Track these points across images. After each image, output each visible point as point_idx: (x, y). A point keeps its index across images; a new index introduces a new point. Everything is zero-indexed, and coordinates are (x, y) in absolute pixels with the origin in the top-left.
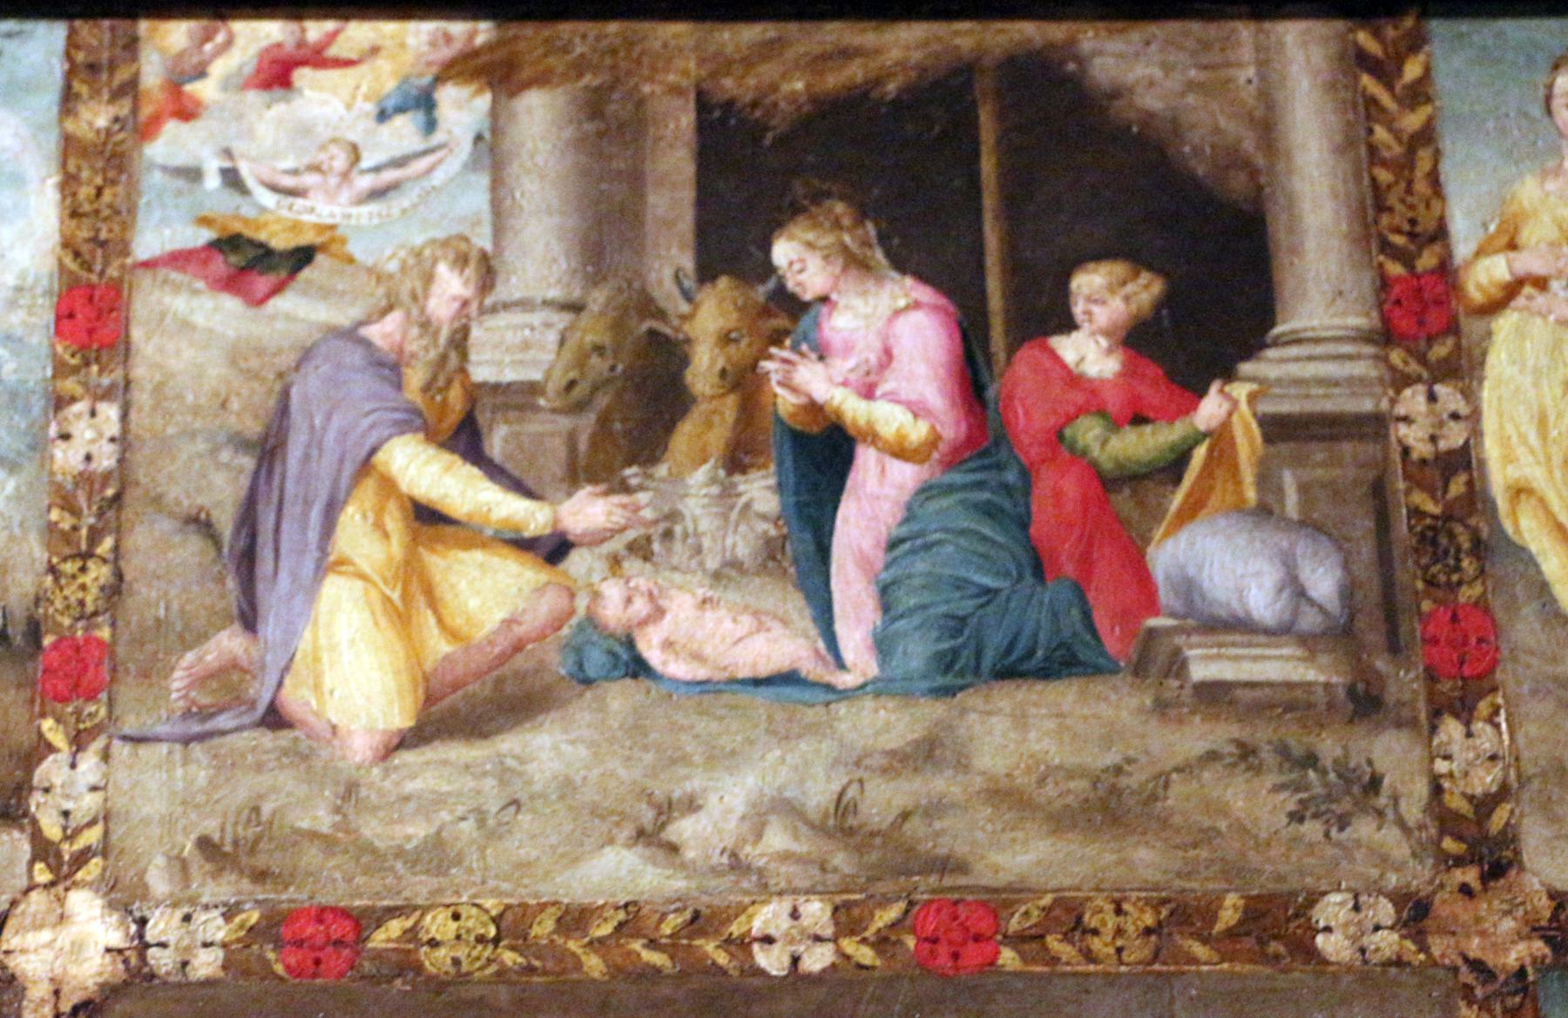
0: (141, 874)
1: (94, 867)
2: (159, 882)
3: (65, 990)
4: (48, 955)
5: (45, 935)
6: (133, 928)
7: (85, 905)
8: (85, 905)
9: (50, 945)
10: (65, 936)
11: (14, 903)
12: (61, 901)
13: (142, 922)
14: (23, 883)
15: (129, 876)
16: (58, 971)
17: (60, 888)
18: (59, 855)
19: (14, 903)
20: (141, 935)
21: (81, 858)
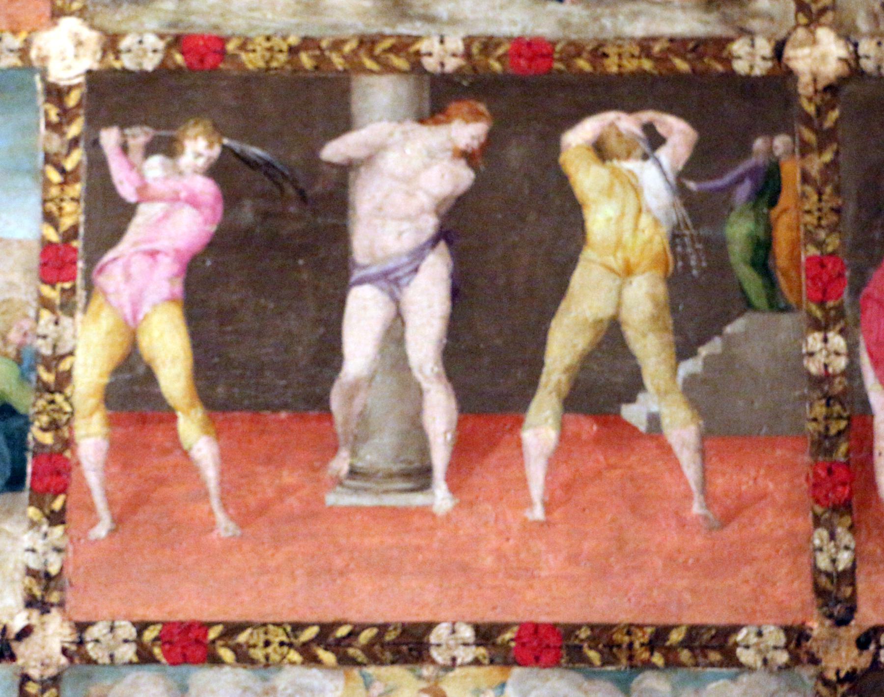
0: (854, 21)
1: (829, 16)
2: (863, 24)
3: (819, 79)
4: (809, 61)
5: (806, 51)
6: (851, 48)
7: (826, 36)
8: (826, 36)
9: (810, 55)
10: (817, 51)
11: (789, 34)
12: (813, 33)
13: (856, 45)
14: (792, 23)
15: (847, 22)
16: (814, 69)
17: (812, 27)
18: (810, 11)
19: (789, 34)
20: (856, 51)
21: (823, 11)
